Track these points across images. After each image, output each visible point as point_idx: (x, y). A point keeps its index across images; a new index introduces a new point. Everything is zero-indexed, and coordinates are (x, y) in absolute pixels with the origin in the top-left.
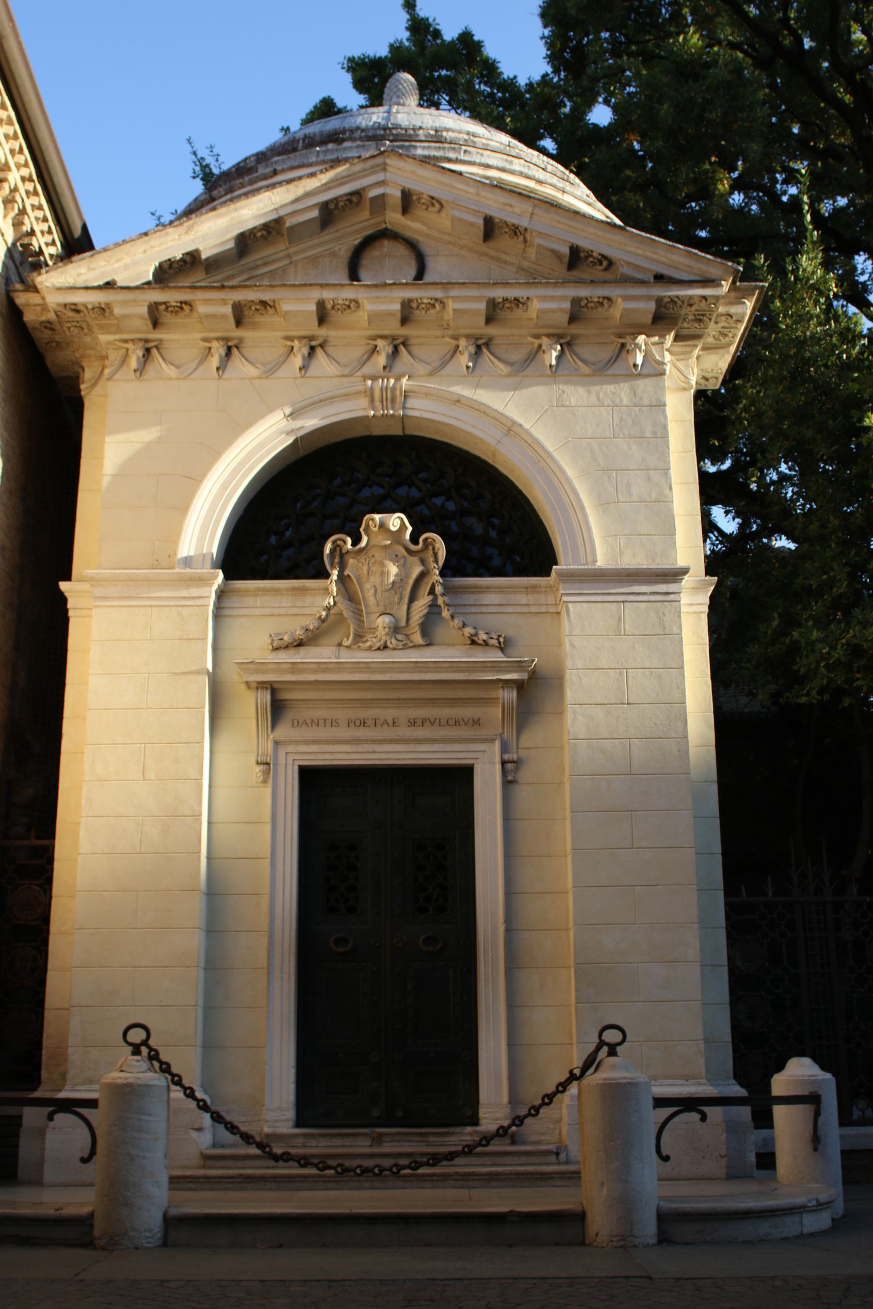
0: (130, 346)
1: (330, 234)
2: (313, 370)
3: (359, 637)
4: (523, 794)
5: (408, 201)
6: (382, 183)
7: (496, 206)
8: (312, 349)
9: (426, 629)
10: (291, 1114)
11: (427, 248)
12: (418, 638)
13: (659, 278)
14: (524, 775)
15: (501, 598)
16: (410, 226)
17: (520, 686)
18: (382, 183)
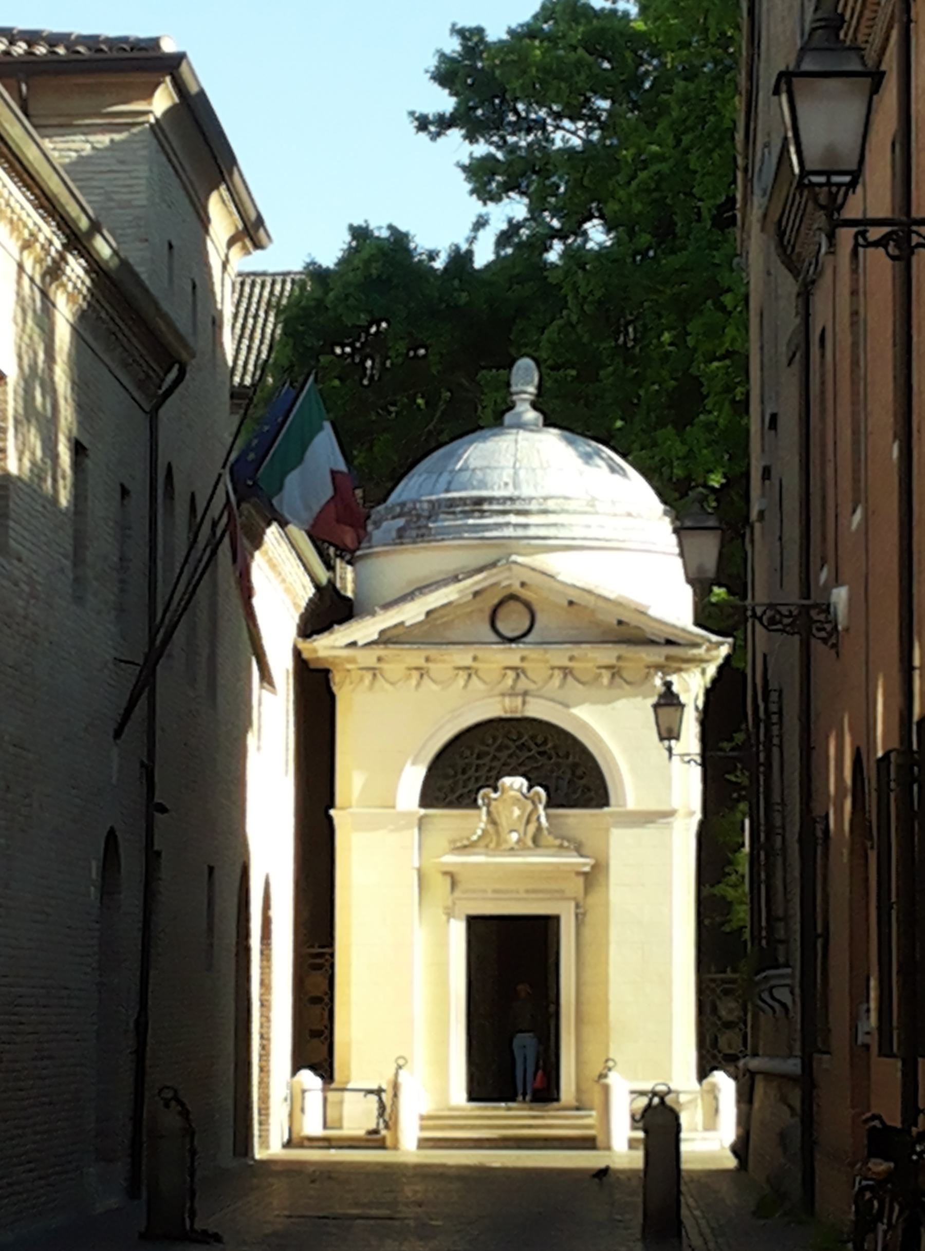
0: (364, 672)
1: (478, 598)
2: (470, 687)
3: (498, 844)
4: (587, 932)
5: (523, 584)
6: (508, 578)
7: (574, 595)
8: (470, 676)
9: (535, 840)
10: (464, 1095)
11: (537, 607)
12: (530, 843)
13: (669, 642)
14: (589, 919)
15: (577, 818)
16: (524, 593)
17: (585, 874)
18: (508, 578)
